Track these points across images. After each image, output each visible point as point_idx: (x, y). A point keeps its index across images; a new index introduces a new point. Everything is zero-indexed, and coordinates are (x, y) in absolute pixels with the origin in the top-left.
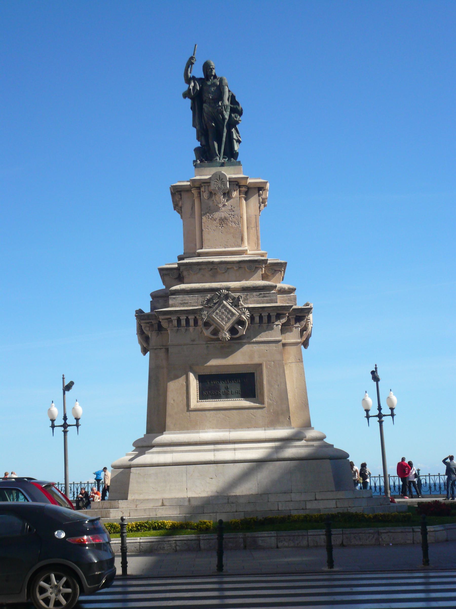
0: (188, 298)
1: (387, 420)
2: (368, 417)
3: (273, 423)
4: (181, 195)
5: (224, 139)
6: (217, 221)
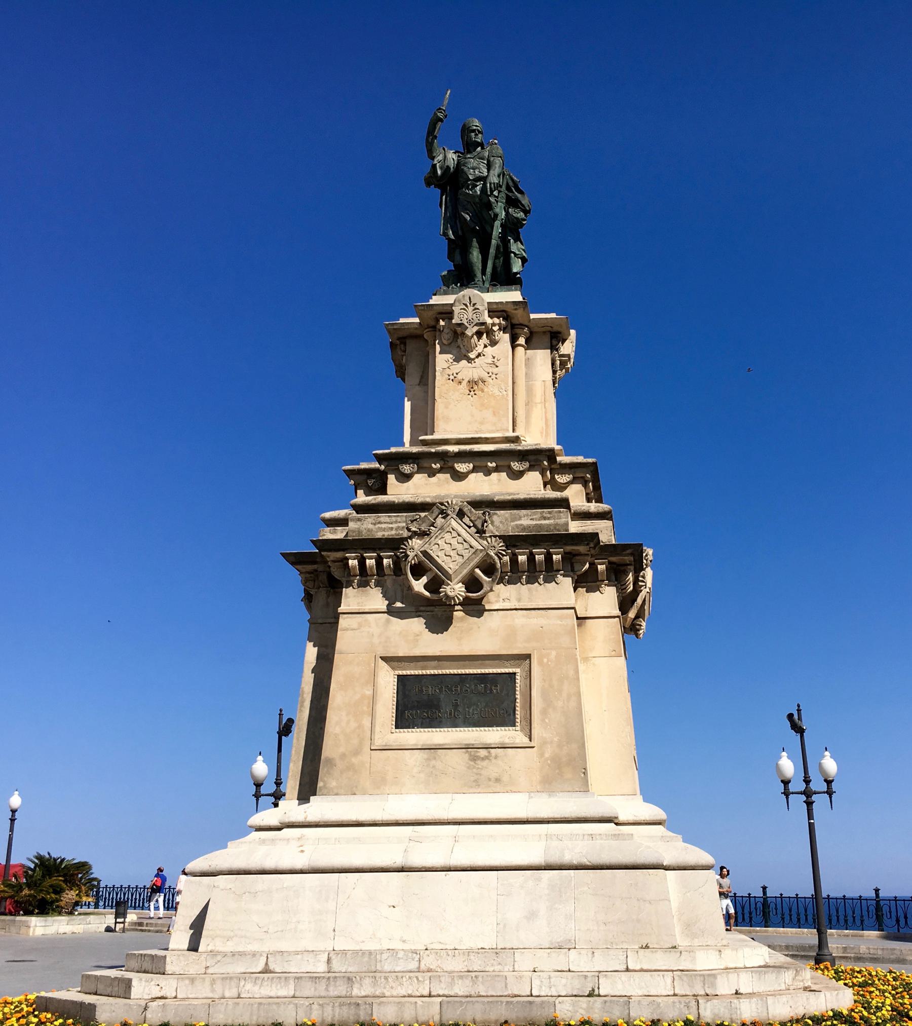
0: (388, 520)
1: (820, 801)
2: (787, 794)
3: (549, 783)
4: (405, 344)
5: (492, 251)
6: (464, 383)
